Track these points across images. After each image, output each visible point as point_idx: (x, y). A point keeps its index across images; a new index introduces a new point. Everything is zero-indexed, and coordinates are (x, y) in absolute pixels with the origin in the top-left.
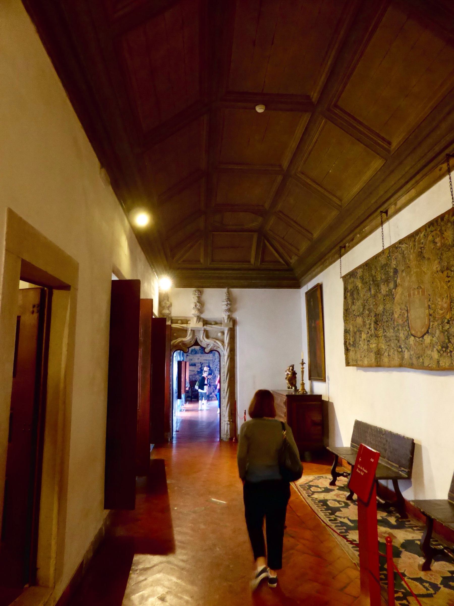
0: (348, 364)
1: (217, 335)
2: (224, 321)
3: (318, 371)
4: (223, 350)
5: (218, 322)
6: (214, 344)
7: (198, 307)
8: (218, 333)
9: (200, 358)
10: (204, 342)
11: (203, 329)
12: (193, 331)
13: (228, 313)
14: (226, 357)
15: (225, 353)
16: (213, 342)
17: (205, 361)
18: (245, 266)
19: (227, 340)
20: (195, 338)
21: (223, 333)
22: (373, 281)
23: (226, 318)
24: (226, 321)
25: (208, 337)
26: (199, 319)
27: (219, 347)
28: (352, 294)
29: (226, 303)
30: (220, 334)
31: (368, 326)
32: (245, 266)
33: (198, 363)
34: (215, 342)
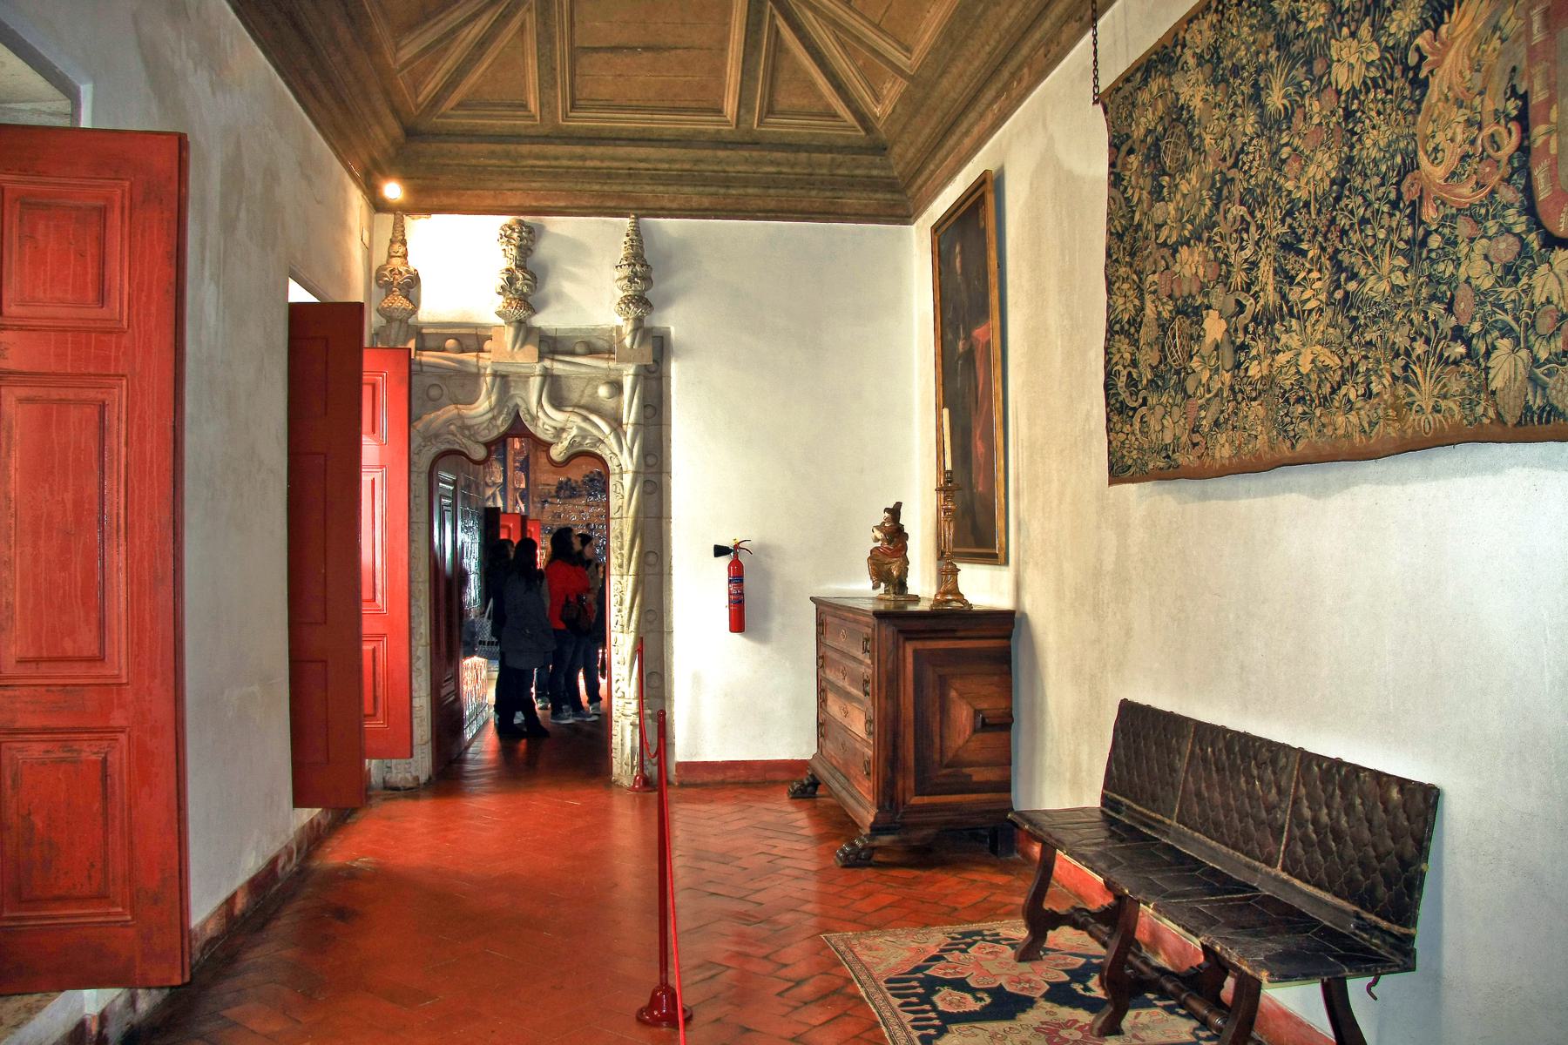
0: (1119, 472)
1: (594, 394)
2: (621, 341)
3: (974, 527)
4: (616, 450)
5: (601, 344)
6: (580, 428)
7: (519, 285)
8: (596, 387)
10: (548, 420)
11: (538, 368)
12: (503, 380)
14: (628, 479)
15: (623, 461)
16: (578, 420)
19: (629, 417)
20: (511, 404)
21: (617, 387)
22: (1282, 43)
23: (627, 328)
24: (628, 341)
25: (558, 402)
26: (525, 332)
28: (1154, 154)
29: (626, 271)
30: (603, 391)
31: (1239, 278)
34: (586, 419)
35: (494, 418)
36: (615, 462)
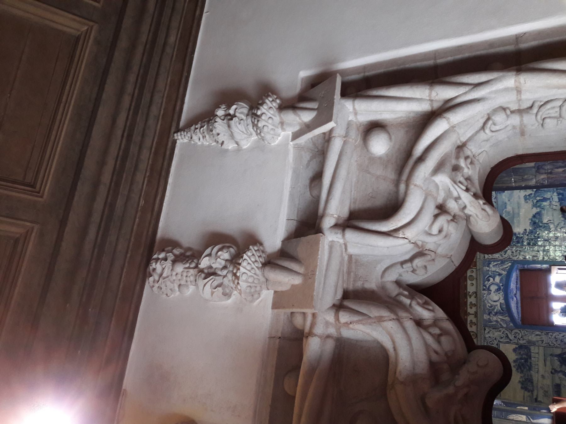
1: (383, 161)
6: (438, 169)
7: (218, 264)
8: (373, 159)
9: (542, 371)
13: (268, 109)
17: (548, 363)
18: (88, 50)
21: (374, 127)
24: (307, 117)
25: (391, 208)
27: (461, 148)
32: (88, 50)
33: (553, 380)
34: (421, 159)
35: (419, 323)
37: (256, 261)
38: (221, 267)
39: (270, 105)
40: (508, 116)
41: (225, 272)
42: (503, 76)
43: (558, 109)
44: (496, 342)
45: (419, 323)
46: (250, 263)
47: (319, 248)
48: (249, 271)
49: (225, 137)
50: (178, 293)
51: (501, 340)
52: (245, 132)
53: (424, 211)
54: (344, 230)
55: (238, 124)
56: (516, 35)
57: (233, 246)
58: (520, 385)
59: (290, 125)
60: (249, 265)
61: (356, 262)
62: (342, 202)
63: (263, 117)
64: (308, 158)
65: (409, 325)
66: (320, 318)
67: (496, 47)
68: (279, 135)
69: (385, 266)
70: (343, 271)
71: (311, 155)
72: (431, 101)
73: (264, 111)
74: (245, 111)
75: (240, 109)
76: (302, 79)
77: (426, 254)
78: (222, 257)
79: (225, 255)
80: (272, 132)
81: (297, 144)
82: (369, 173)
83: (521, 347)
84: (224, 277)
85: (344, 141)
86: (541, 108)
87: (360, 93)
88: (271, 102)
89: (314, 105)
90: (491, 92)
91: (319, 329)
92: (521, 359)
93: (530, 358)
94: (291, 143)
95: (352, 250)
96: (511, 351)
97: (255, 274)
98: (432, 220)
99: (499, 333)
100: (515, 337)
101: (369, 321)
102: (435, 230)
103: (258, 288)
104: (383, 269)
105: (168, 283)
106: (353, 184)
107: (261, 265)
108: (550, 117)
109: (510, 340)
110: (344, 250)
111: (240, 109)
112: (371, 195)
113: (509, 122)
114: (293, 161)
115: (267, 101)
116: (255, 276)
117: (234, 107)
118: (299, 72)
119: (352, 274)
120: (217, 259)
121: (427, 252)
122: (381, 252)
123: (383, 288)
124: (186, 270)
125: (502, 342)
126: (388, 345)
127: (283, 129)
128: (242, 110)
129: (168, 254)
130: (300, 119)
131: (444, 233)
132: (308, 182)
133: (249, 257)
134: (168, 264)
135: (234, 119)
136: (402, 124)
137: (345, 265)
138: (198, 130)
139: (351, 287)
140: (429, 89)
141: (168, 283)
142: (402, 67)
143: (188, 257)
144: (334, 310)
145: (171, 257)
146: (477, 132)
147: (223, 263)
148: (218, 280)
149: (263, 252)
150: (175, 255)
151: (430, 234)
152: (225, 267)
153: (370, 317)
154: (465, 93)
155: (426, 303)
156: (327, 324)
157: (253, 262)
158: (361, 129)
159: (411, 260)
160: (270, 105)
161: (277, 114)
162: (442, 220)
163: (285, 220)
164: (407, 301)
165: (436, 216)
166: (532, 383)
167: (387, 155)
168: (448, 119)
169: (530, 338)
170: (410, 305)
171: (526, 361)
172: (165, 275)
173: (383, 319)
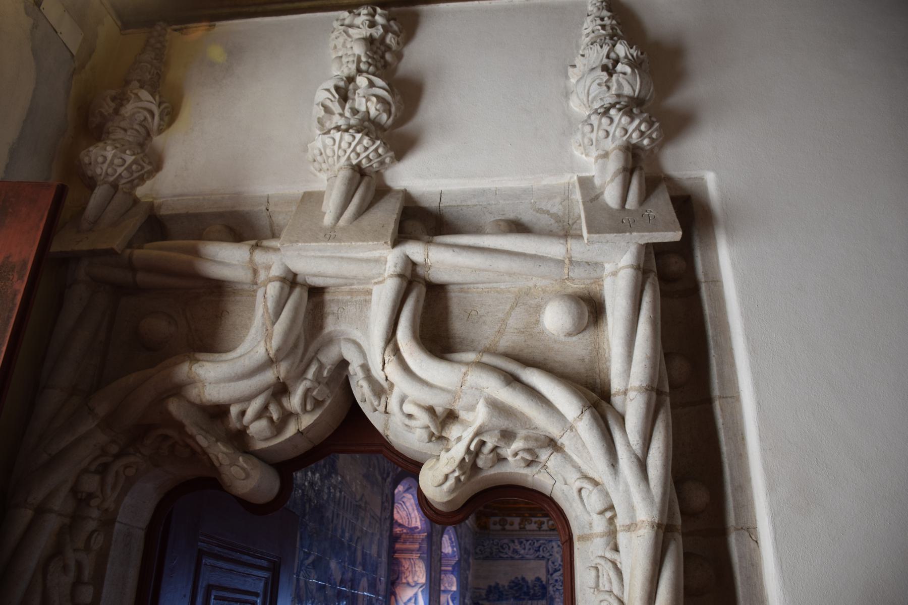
4: (598, 465)
6: (496, 407)
7: (360, 103)
14: (636, 550)
20: (329, 357)
24: (611, 196)
27: (552, 444)
34: (512, 380)
35: (280, 390)
36: (594, 501)
37: (358, 155)
38: (356, 107)
39: (631, 128)
40: (602, 513)
41: (347, 113)
42: (652, 502)
43: (607, 589)
44: (547, 555)
45: (280, 390)
46: (365, 149)
47: (368, 241)
48: (340, 147)
49: (582, 68)
50: (334, 57)
51: (550, 562)
52: (590, 98)
53: (426, 389)
54: (401, 276)
55: (598, 81)
56: (755, 528)
57: (391, 118)
58: (493, 584)
59: (603, 169)
60: (347, 145)
61: (365, 301)
62: (456, 268)
63: (605, 121)
64: (554, 210)
65: (269, 377)
66: (273, 257)
67: (734, 496)
68: (587, 155)
69: (361, 343)
70: (352, 284)
71: (560, 214)
72: (625, 393)
73: (616, 120)
74: (627, 90)
75: (627, 83)
76: (702, 179)
77: (380, 398)
78: (369, 104)
79: (373, 108)
80: (586, 141)
81: (574, 187)
82: (512, 308)
83: (544, 588)
84: (342, 115)
85: (563, 262)
86: (610, 564)
87: (653, 279)
88: (638, 128)
89: (632, 201)
90: (627, 485)
91: (260, 257)
92: (528, 587)
93: (530, 599)
94: (576, 178)
95: (376, 290)
96: (537, 575)
97: (339, 157)
98: (422, 404)
99: (560, 559)
100: (556, 581)
101: (268, 323)
102: (409, 408)
103: (324, 166)
104: (358, 340)
105: (341, 40)
106: (495, 285)
107: (354, 162)
108: (598, 576)
109: (552, 575)
110: (376, 280)
111: (627, 83)
112: (473, 313)
113: (596, 518)
114: (545, 186)
115: (637, 122)
116: (336, 157)
117: (628, 70)
118: (713, 170)
119: (349, 297)
120: (368, 100)
121: (383, 400)
122: (366, 333)
123: (330, 341)
124: (355, 59)
125: (547, 563)
126: (240, 351)
127: (597, 158)
128: (625, 83)
129: (380, 27)
130: (609, 182)
131: (407, 421)
132: (511, 216)
133: (359, 142)
134: (365, 32)
135: (605, 73)
136: (598, 352)
137: (361, 287)
138: (599, 22)
139: (328, 297)
140: (640, 387)
141: (341, 40)
142: (712, 343)
143: (383, 57)
144: (283, 275)
145: (378, 32)
146: (578, 469)
147: (363, 108)
148: (336, 107)
149: (382, 163)
150: (383, 39)
151: (402, 402)
152: (355, 112)
153: (274, 324)
154: (628, 444)
155: (318, 404)
156: (268, 268)
157: (354, 150)
158: (595, 288)
159: (369, 377)
160: (631, 128)
161: (618, 142)
162: (423, 418)
163: (440, 189)
164: (310, 374)
165: (431, 410)
166: (498, 600)
167: (542, 332)
168: (580, 417)
169: (557, 600)
170: (306, 379)
171: (527, 594)
172: (351, 31)
173: (268, 340)
